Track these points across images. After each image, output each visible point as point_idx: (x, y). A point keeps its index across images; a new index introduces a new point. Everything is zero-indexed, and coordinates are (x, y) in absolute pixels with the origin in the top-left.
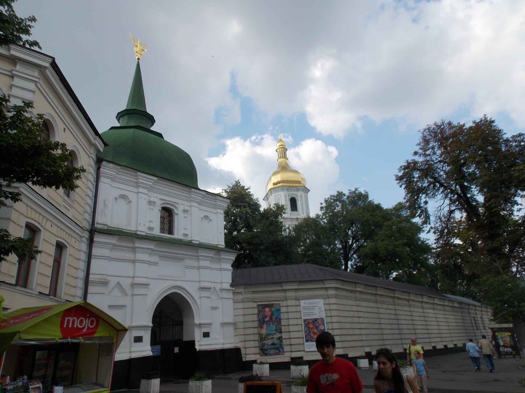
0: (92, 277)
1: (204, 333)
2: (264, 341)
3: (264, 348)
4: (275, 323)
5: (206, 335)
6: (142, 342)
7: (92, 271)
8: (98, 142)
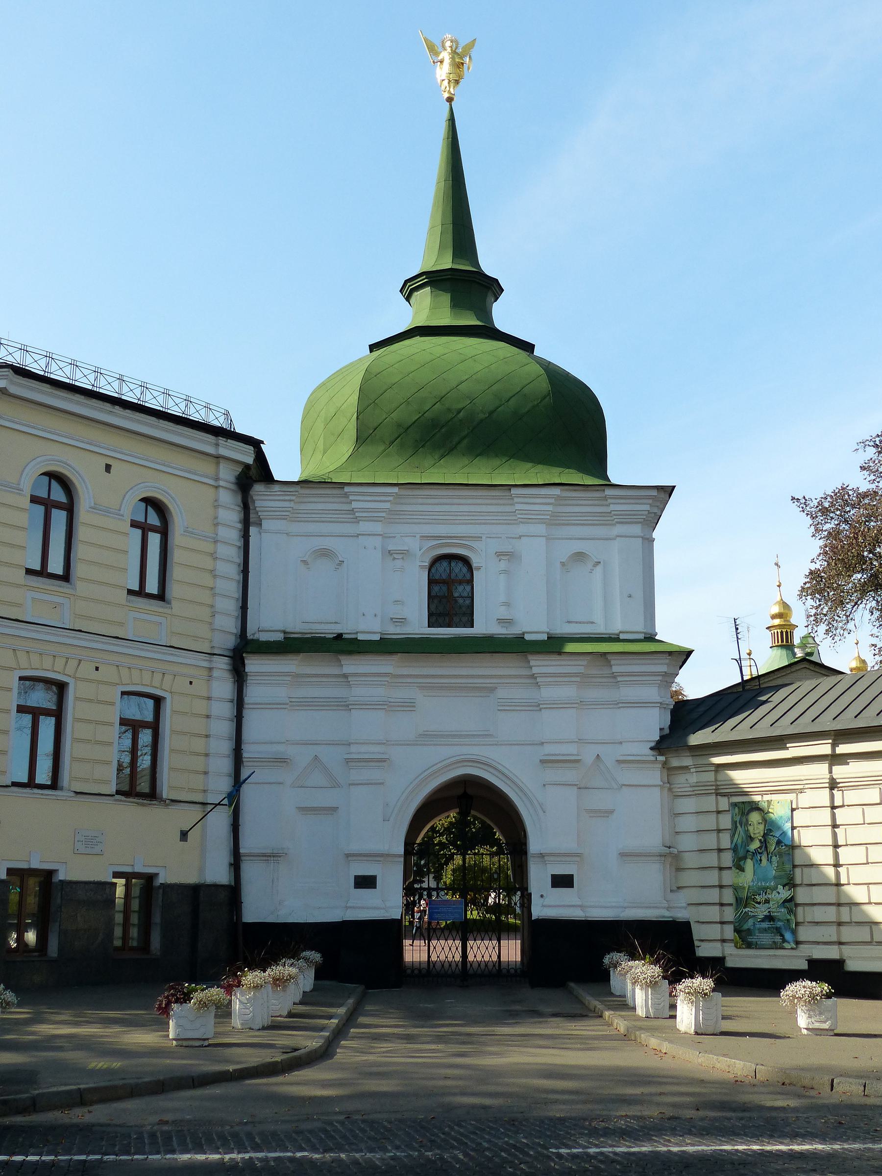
0: (248, 751)
1: (553, 876)
2: (745, 908)
3: (745, 927)
4: (774, 858)
5: (563, 881)
6: (355, 888)
7: (246, 735)
8: (226, 447)
